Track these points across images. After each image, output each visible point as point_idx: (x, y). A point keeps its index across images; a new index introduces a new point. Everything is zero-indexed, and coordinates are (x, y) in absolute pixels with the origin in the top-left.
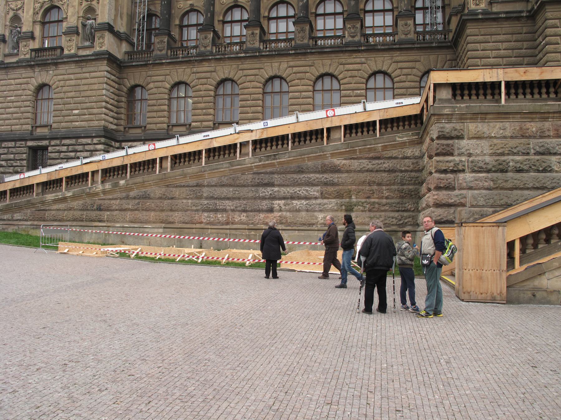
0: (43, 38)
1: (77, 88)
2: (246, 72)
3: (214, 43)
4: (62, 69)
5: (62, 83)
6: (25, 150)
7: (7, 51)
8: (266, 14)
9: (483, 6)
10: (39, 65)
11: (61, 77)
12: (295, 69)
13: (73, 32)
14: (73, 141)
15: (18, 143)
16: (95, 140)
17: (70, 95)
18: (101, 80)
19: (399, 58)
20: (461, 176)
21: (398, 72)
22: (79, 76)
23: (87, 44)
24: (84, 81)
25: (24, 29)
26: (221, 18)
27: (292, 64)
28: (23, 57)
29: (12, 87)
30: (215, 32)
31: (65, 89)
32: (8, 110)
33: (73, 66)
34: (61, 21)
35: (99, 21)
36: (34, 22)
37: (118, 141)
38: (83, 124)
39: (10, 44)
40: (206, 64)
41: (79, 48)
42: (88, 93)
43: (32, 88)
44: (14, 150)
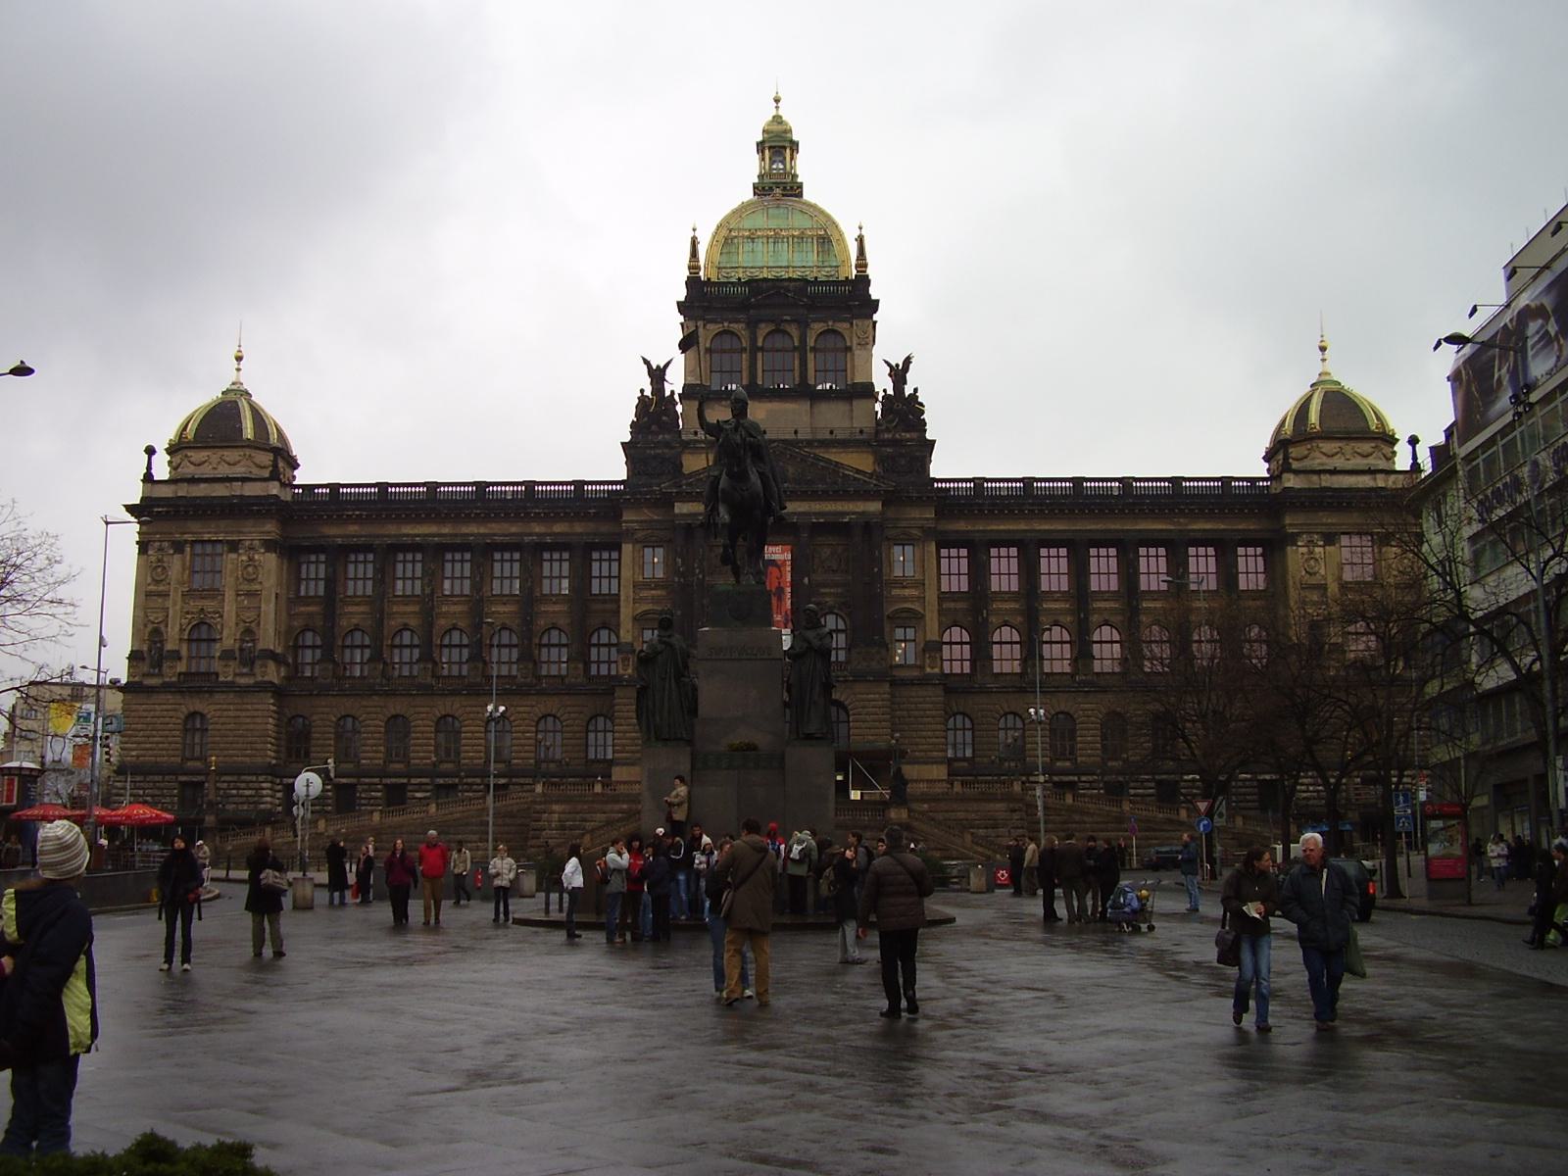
0: (190, 658)
1: (237, 720)
2: (418, 709)
3: (383, 674)
4: (217, 696)
5: (218, 713)
6: (176, 785)
7: (145, 669)
8: (439, 642)
9: (630, 671)
10: (190, 692)
11: (219, 706)
12: (468, 709)
13: (227, 655)
14: (235, 778)
15: (167, 778)
16: (261, 778)
17: (229, 727)
18: (266, 713)
19: (569, 703)
20: (544, 833)
21: (566, 716)
22: (239, 707)
23: (245, 670)
24: (244, 714)
25: (169, 646)
26: (389, 642)
27: (465, 703)
28: (167, 680)
29: (157, 713)
30: (385, 663)
31: (222, 720)
32: (151, 739)
33: (232, 696)
34: (214, 640)
35: (261, 646)
36: (181, 639)
37: (277, 777)
38: (247, 759)
39: (148, 661)
40: (376, 698)
41: (236, 675)
42: (251, 727)
43: (183, 717)
44: (162, 785)
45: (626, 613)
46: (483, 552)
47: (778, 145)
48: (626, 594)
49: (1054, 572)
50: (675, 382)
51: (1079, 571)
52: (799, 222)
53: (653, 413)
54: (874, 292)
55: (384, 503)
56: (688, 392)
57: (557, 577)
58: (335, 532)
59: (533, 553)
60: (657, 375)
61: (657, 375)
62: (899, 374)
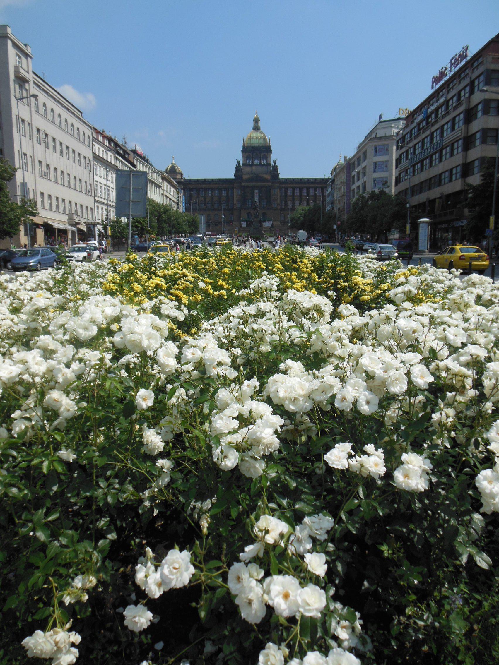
45: (235, 199)
46: (213, 190)
47: (256, 121)
48: (235, 196)
49: (297, 193)
50: (241, 163)
51: (301, 192)
52: (259, 135)
53: (238, 169)
54: (272, 148)
55: (198, 182)
56: (243, 164)
57: (224, 193)
58: (190, 186)
59: (220, 189)
60: (239, 162)
61: (239, 162)
62: (275, 162)
